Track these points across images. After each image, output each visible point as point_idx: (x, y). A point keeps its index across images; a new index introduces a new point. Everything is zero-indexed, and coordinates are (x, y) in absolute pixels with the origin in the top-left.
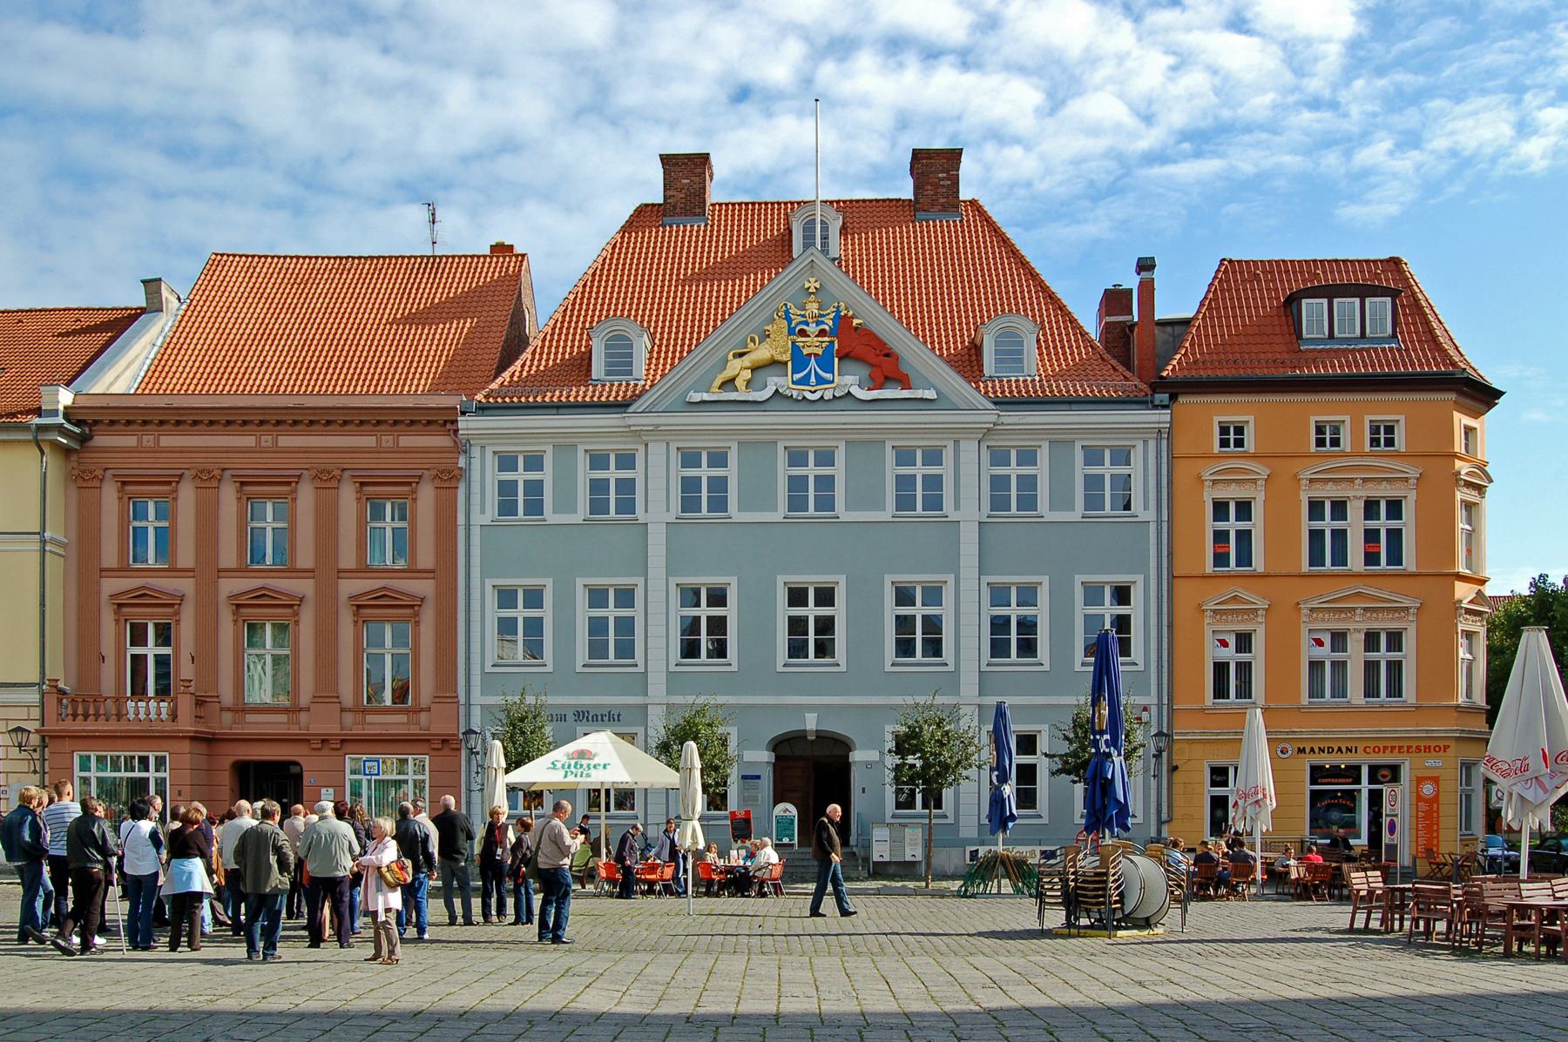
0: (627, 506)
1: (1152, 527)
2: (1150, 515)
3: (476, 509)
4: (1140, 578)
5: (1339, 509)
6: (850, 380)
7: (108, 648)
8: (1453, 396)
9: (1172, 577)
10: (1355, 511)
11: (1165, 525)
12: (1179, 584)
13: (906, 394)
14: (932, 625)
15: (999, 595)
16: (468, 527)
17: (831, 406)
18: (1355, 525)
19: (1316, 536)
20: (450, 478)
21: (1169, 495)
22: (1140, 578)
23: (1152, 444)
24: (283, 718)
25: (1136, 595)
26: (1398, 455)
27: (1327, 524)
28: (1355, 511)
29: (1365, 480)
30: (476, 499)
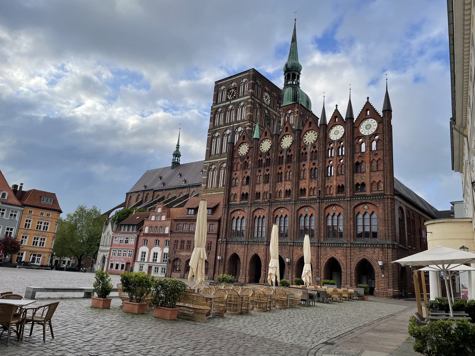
1: (18, 222)
2: (18, 220)
4: (15, 228)
5: (41, 223)
8: (57, 212)
9: (19, 228)
10: (43, 223)
12: (19, 229)
19: (38, 226)
21: (21, 218)
22: (15, 228)
23: (20, 212)
25: (14, 230)
26: (49, 218)
27: (39, 224)
28: (43, 223)
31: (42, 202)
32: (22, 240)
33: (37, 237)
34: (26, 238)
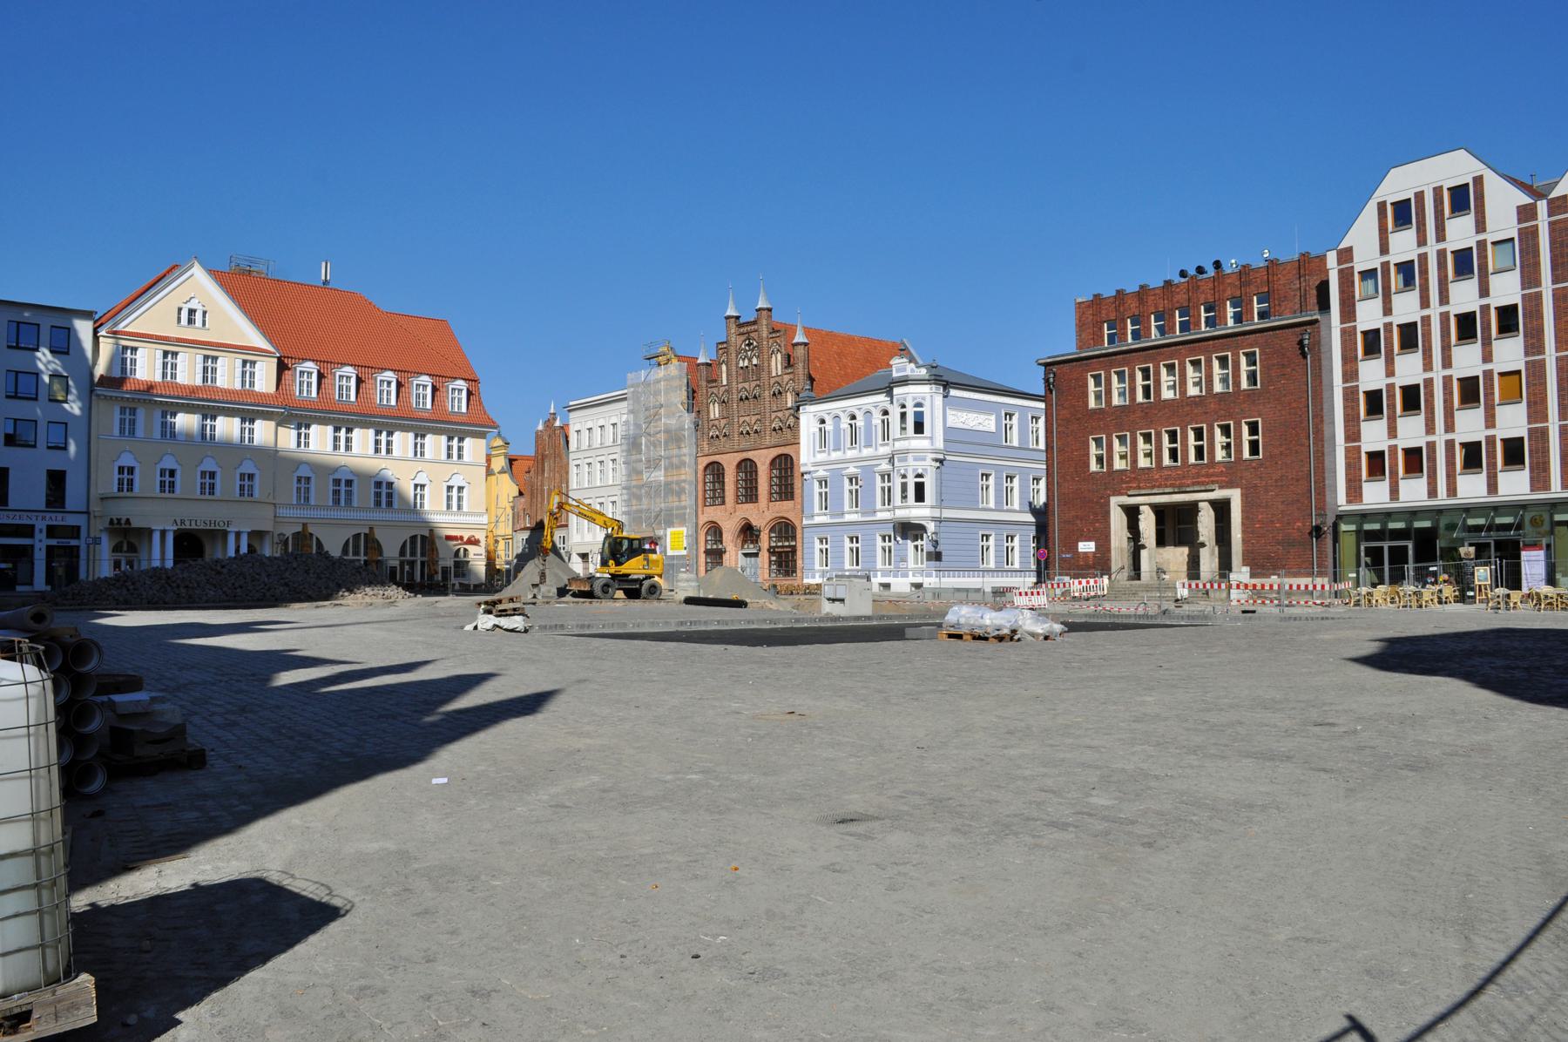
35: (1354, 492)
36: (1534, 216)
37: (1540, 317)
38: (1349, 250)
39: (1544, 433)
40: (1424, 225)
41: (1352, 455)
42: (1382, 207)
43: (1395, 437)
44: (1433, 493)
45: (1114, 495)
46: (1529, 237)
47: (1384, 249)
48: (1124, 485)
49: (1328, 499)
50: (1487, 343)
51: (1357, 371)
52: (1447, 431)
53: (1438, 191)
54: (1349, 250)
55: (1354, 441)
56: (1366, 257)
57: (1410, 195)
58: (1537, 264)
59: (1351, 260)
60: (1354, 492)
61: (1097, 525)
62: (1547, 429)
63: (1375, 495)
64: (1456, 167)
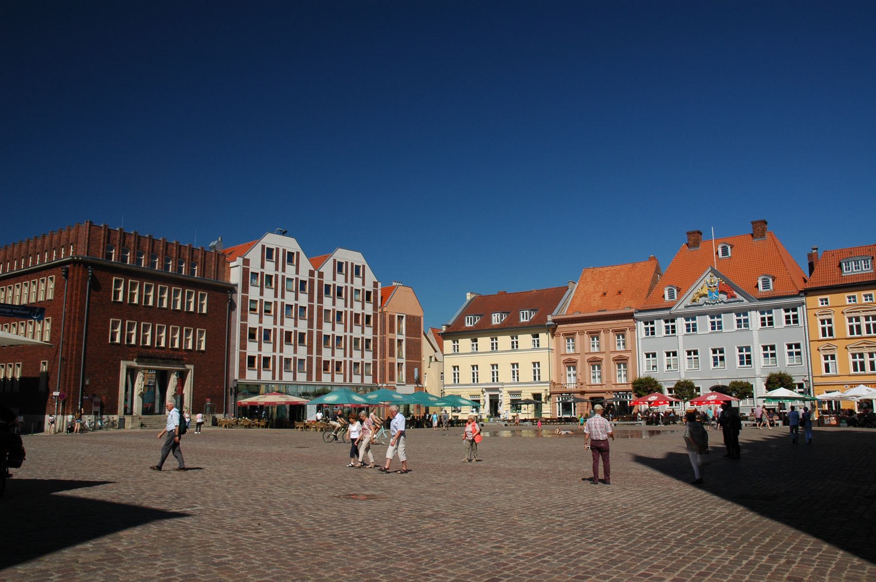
0: (673, 332)
3: (639, 335)
6: (723, 297)
7: (563, 372)
9: (810, 341)
11: (807, 328)
13: (736, 300)
14: (748, 357)
15: (765, 348)
16: (638, 339)
17: (719, 304)
18: (863, 323)
20: (633, 329)
24: (600, 386)
29: (863, 311)
30: (639, 333)
31: (845, 273)
32: (827, 366)
33: (856, 351)
34: (833, 357)
35: (242, 374)
36: (314, 276)
37: (313, 314)
38: (248, 260)
39: (312, 358)
40: (278, 262)
41: (242, 355)
42: (263, 247)
43: (261, 351)
44: (274, 378)
45: (123, 360)
46: (312, 282)
47: (262, 266)
48: (131, 355)
49: (231, 375)
50: (296, 319)
51: (247, 317)
52: (280, 352)
53: (284, 250)
54: (248, 260)
55: (244, 349)
56: (255, 267)
57: (274, 247)
58: (313, 294)
59: (249, 265)
60: (242, 374)
61: (110, 378)
62: (312, 357)
63: (251, 376)
64: (290, 244)
